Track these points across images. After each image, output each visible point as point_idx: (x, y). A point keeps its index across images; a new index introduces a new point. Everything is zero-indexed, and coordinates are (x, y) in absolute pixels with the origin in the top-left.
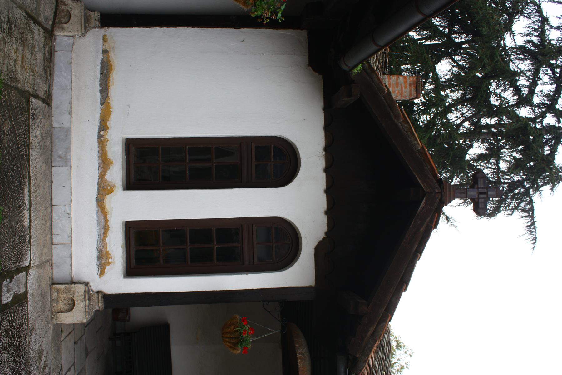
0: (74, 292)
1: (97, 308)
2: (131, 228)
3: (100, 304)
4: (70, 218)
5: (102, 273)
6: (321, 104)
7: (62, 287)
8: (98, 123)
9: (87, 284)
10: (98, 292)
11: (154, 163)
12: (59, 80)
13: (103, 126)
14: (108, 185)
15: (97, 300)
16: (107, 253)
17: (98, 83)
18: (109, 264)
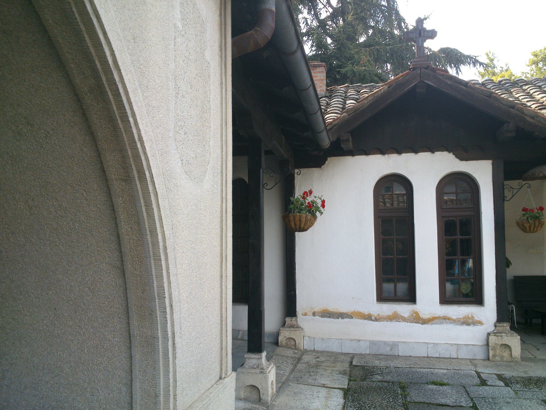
0: (496, 344)
1: (508, 327)
2: (445, 300)
3: (505, 325)
4: (437, 344)
5: (480, 323)
6: (349, 160)
8: (366, 321)
9: (489, 334)
10: (495, 326)
12: (335, 348)
13: (369, 317)
14: (412, 315)
15: (502, 328)
16: (464, 318)
17: (337, 320)
18: (473, 317)
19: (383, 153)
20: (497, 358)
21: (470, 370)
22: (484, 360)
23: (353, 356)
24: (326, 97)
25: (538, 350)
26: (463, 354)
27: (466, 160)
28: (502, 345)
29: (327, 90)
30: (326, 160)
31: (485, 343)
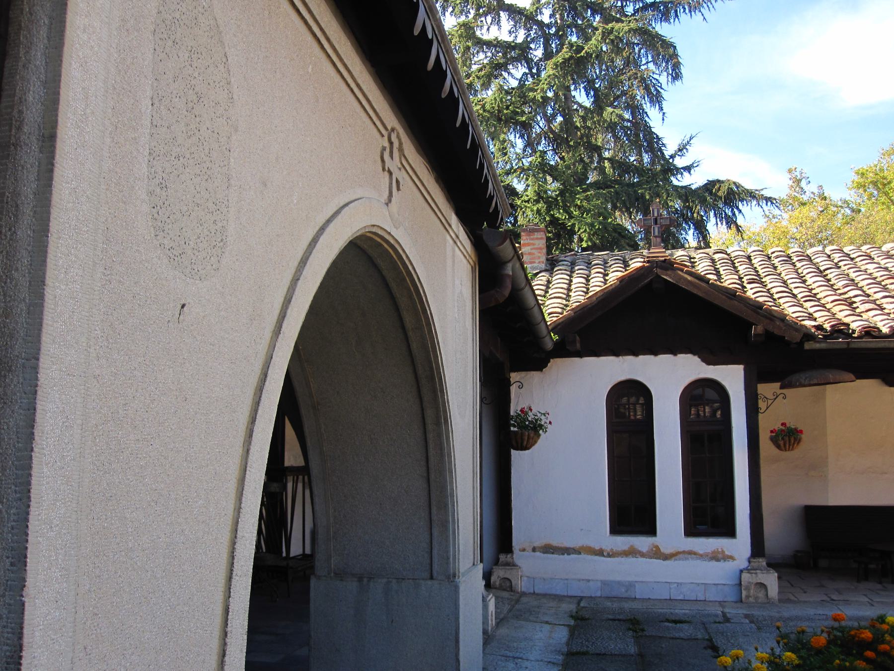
2: (691, 530)
4: (681, 584)
7: (744, 593)
8: (597, 558)
11: (632, 509)
12: (559, 590)
13: (600, 553)
17: (561, 556)
19: (616, 354)
20: (751, 600)
21: (718, 611)
22: (736, 602)
23: (581, 598)
24: (545, 271)
25: (805, 592)
26: (711, 597)
27: (714, 364)
28: (757, 583)
29: (547, 260)
30: (549, 362)
31: (738, 582)
